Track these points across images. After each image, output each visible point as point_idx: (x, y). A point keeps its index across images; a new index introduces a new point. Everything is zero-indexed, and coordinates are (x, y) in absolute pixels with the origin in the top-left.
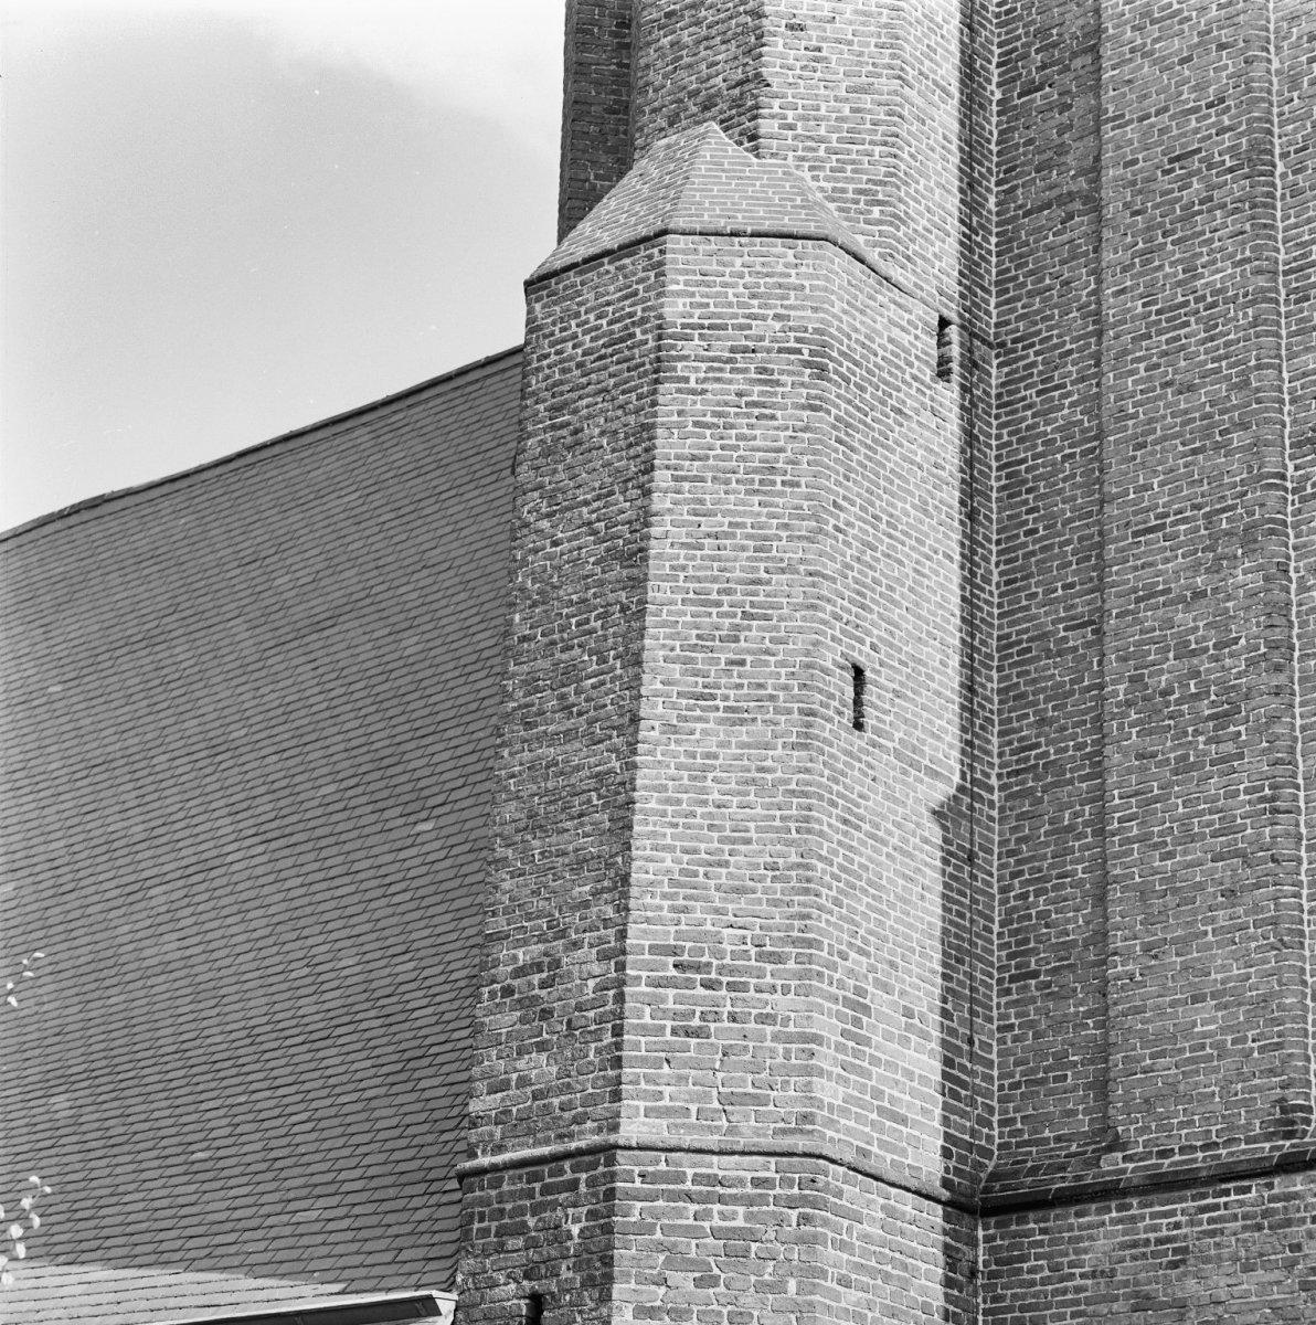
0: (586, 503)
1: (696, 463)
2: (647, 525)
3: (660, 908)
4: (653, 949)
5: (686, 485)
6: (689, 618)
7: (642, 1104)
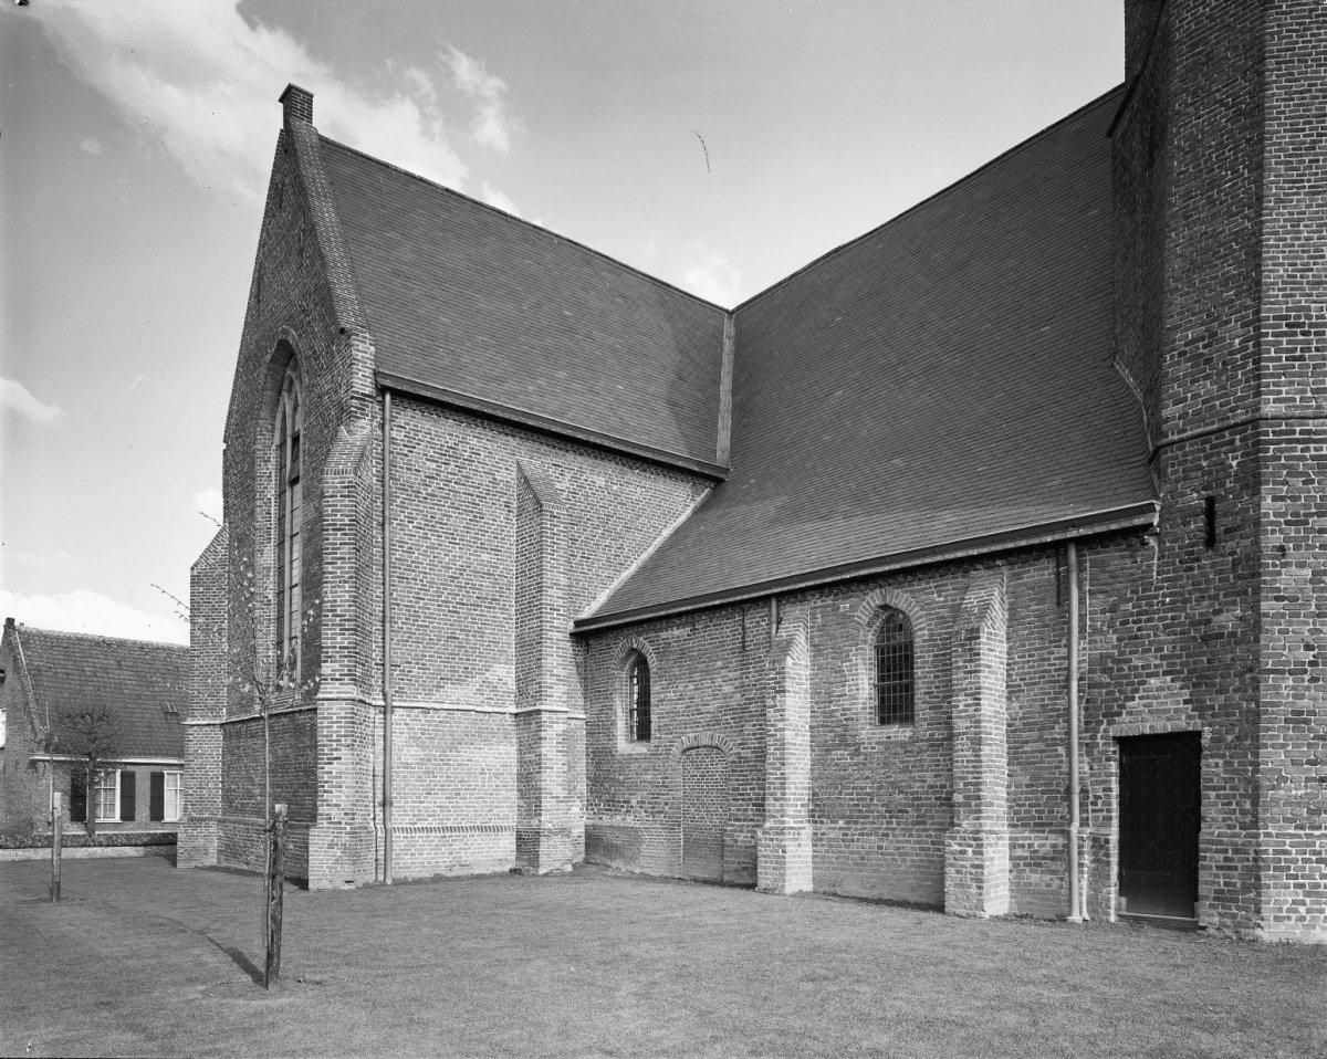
0: (1218, 90)
1: (1288, 53)
2: (1262, 91)
3: (1278, 296)
4: (1275, 318)
5: (1283, 66)
6: (1287, 140)
7: (1271, 397)
